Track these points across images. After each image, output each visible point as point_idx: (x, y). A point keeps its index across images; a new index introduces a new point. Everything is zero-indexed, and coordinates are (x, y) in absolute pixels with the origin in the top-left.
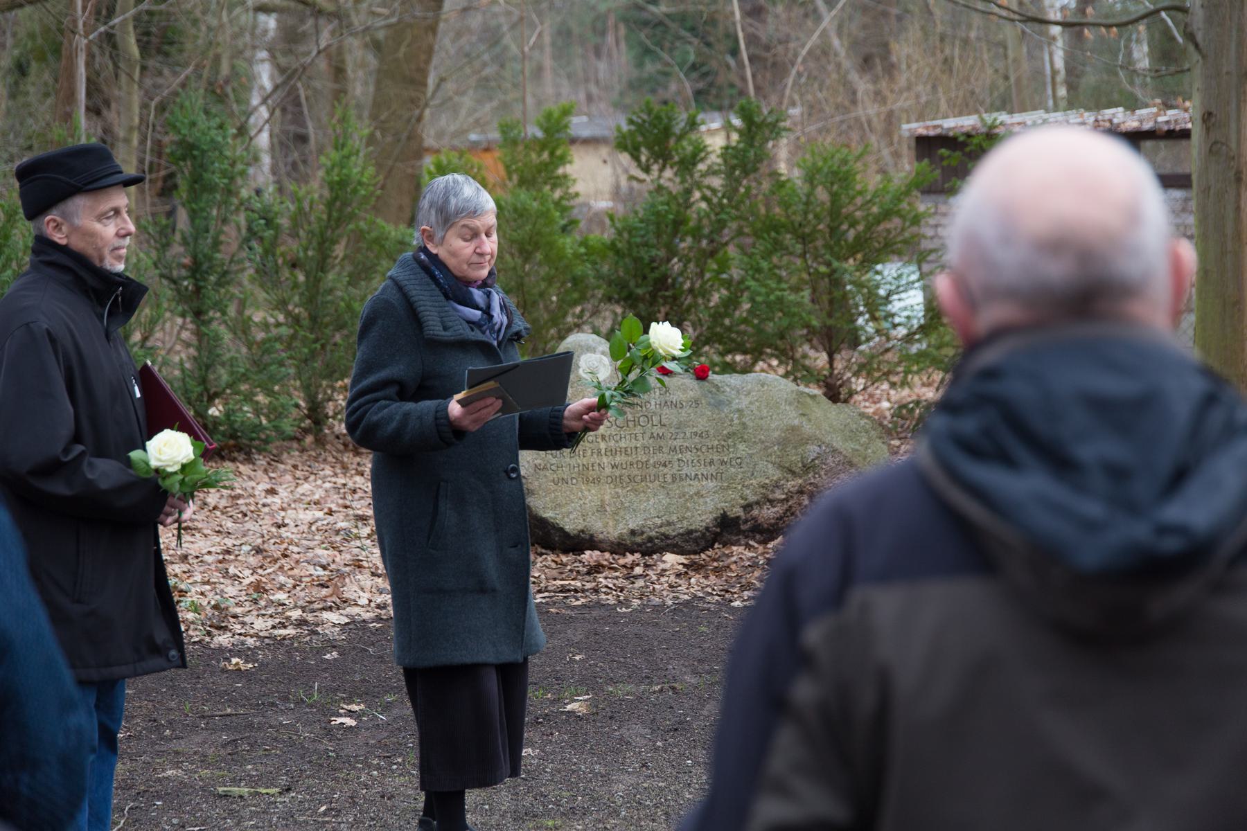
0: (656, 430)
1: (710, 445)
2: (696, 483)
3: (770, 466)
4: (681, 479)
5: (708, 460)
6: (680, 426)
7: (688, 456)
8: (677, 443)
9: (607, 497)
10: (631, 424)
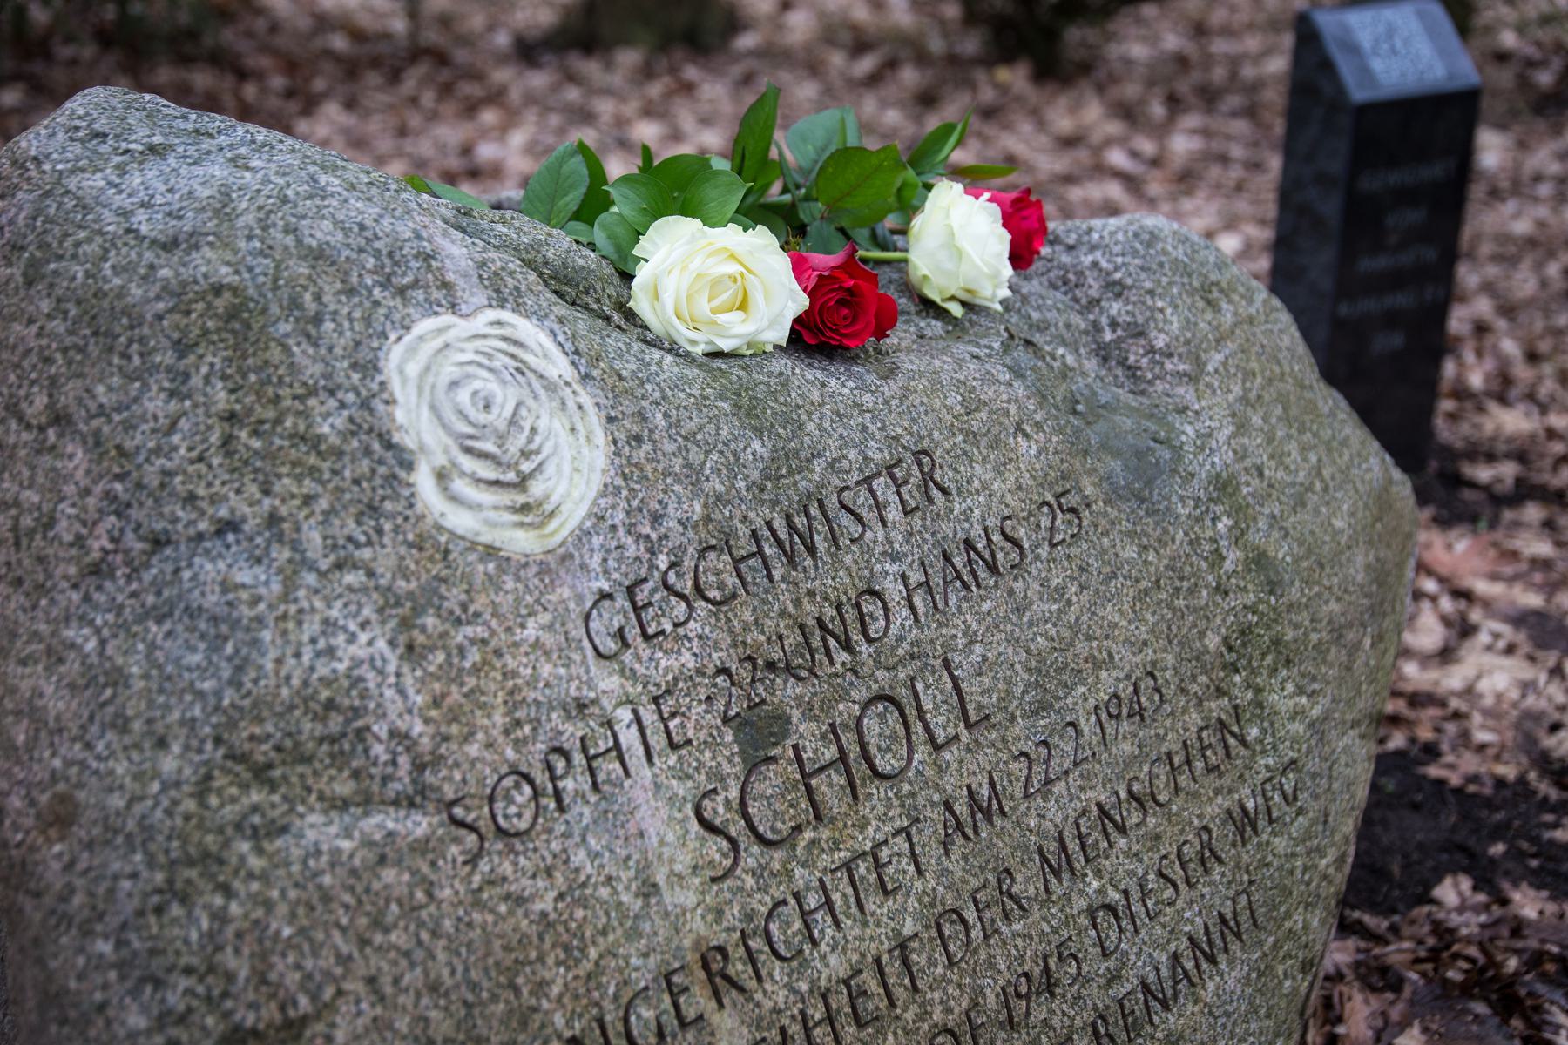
10: (830, 787)
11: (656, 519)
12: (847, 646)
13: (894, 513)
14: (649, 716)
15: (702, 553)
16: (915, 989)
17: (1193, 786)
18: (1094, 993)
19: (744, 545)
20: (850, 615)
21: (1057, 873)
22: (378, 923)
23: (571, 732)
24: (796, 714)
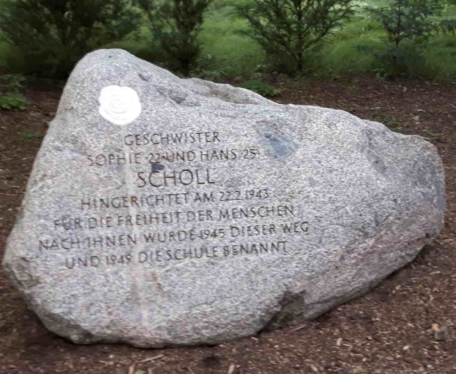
0: (203, 190)
1: (270, 206)
2: (252, 257)
3: (341, 229)
4: (235, 253)
5: (268, 226)
6: (233, 185)
7: (242, 222)
8: (228, 206)
9: (140, 282)
11: (146, 126)
12: (183, 159)
13: (203, 141)
14: (133, 156)
15: (155, 134)
16: (178, 221)
17: (273, 216)
18: (226, 242)
19: (164, 136)
20: (186, 155)
21: (224, 216)
22: (71, 168)
23: (116, 153)
24: (166, 167)
